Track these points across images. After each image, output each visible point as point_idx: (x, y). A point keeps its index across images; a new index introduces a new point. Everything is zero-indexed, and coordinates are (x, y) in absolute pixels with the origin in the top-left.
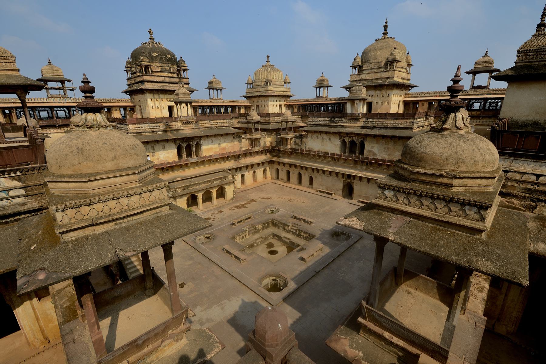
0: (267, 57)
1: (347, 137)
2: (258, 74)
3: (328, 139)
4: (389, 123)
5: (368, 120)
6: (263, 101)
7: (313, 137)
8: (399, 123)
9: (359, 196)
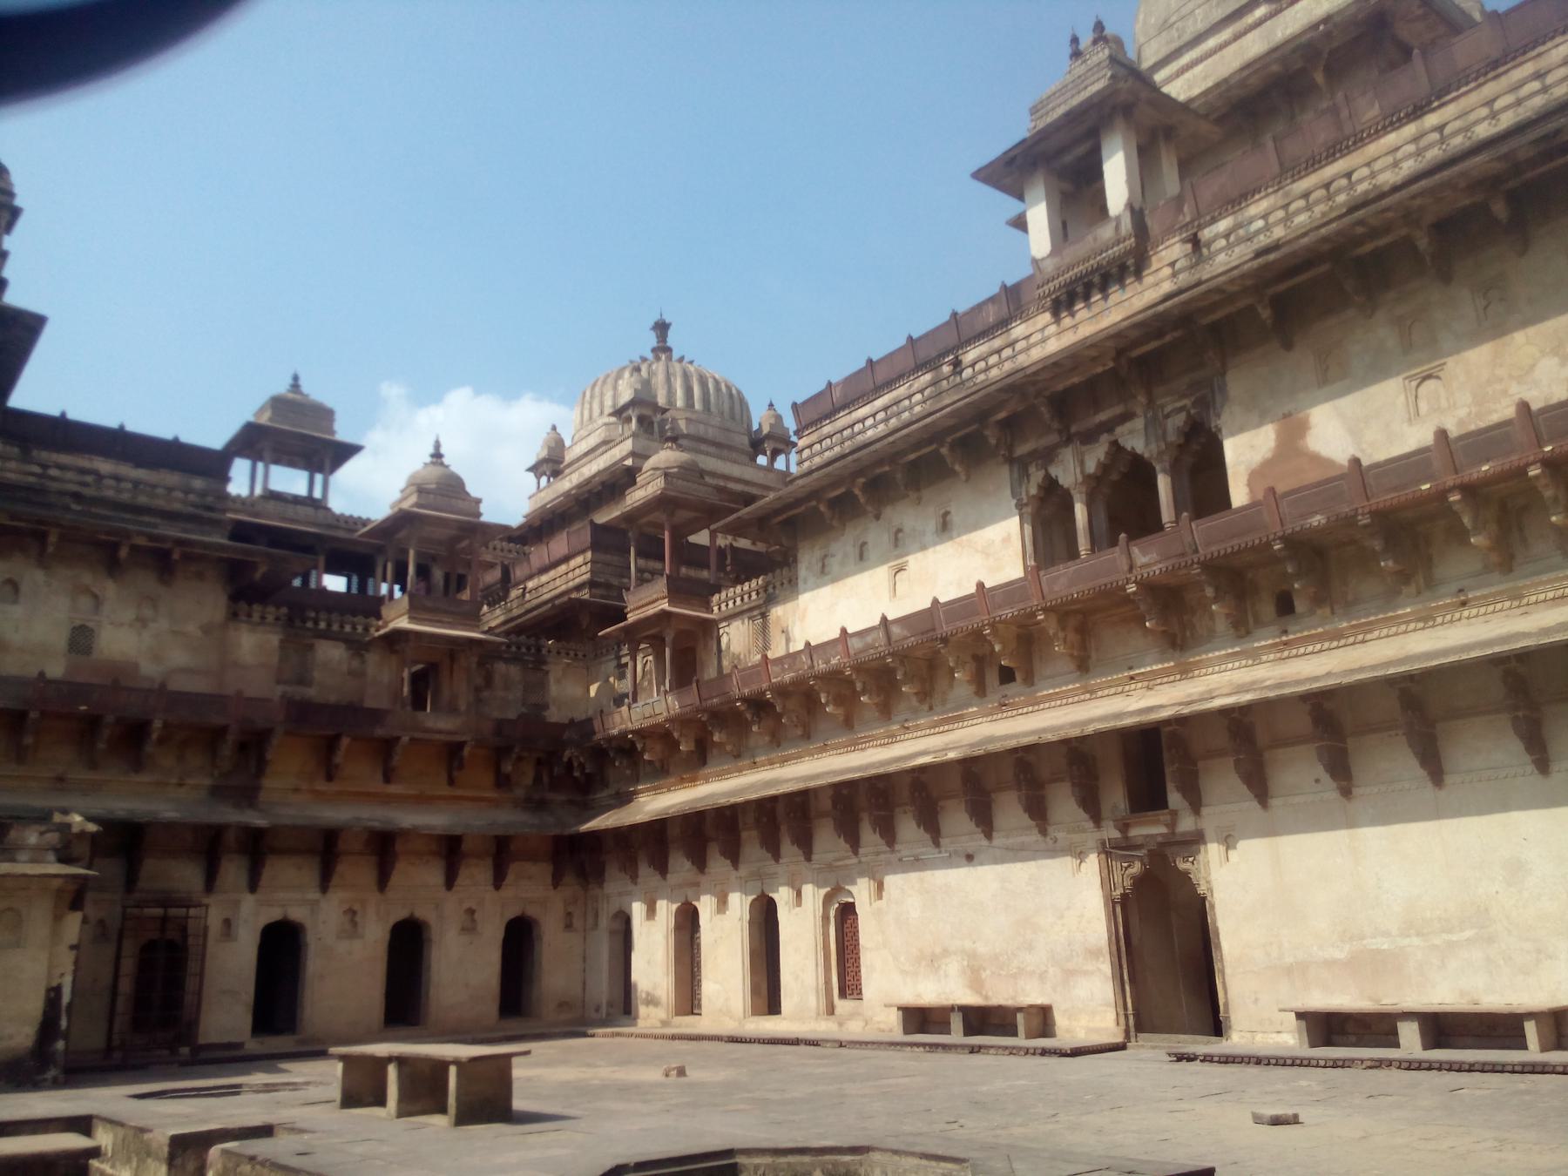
1: (1068, 441)
3: (932, 524)
5: (1206, 234)
7: (834, 564)
8: (1472, 117)
9: (1289, 971)
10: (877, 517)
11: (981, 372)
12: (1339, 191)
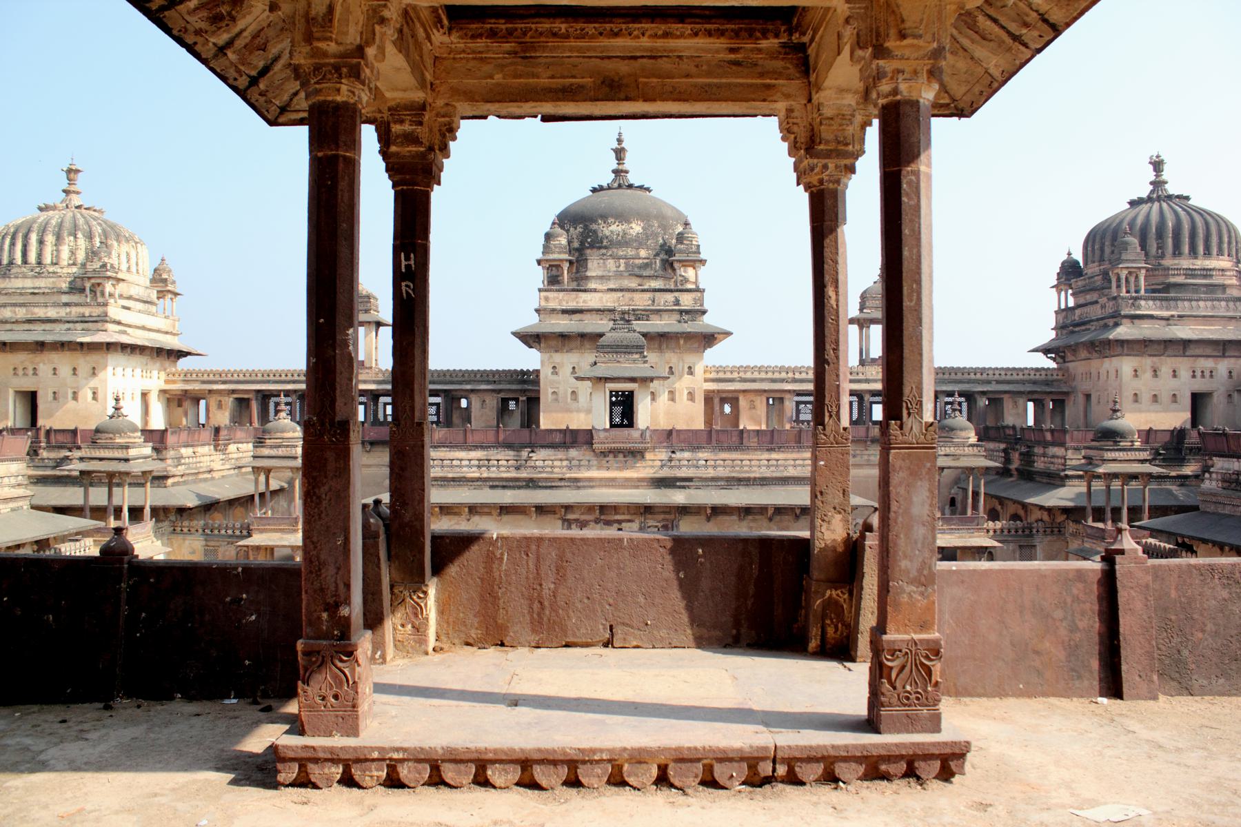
0: (69, 171)
2: (34, 238)
4: (753, 463)
5: (678, 455)
6: (65, 371)
10: (469, 520)
11: (548, 466)
12: (737, 466)
